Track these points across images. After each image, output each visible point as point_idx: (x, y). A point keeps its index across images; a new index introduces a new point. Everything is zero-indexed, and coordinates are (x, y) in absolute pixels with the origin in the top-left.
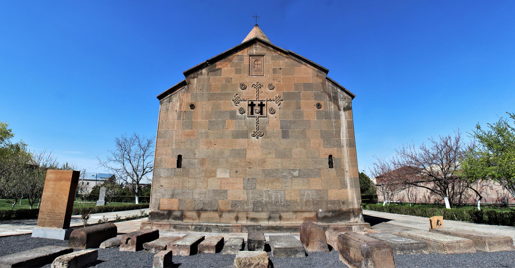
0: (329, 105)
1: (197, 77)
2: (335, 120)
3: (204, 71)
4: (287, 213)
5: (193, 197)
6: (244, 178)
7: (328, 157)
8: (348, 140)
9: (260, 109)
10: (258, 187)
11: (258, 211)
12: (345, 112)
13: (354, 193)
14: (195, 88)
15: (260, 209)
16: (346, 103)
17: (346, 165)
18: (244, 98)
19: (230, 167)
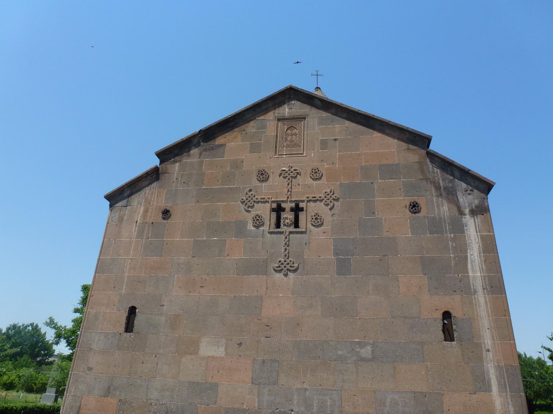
0: (438, 206)
1: (180, 161)
2: (452, 235)
3: (195, 151)
7: (441, 317)
8: (487, 278)
12: (473, 217)
13: (508, 404)
14: (175, 180)
16: (474, 199)
17: (485, 334)
18: (263, 197)
19: (228, 333)
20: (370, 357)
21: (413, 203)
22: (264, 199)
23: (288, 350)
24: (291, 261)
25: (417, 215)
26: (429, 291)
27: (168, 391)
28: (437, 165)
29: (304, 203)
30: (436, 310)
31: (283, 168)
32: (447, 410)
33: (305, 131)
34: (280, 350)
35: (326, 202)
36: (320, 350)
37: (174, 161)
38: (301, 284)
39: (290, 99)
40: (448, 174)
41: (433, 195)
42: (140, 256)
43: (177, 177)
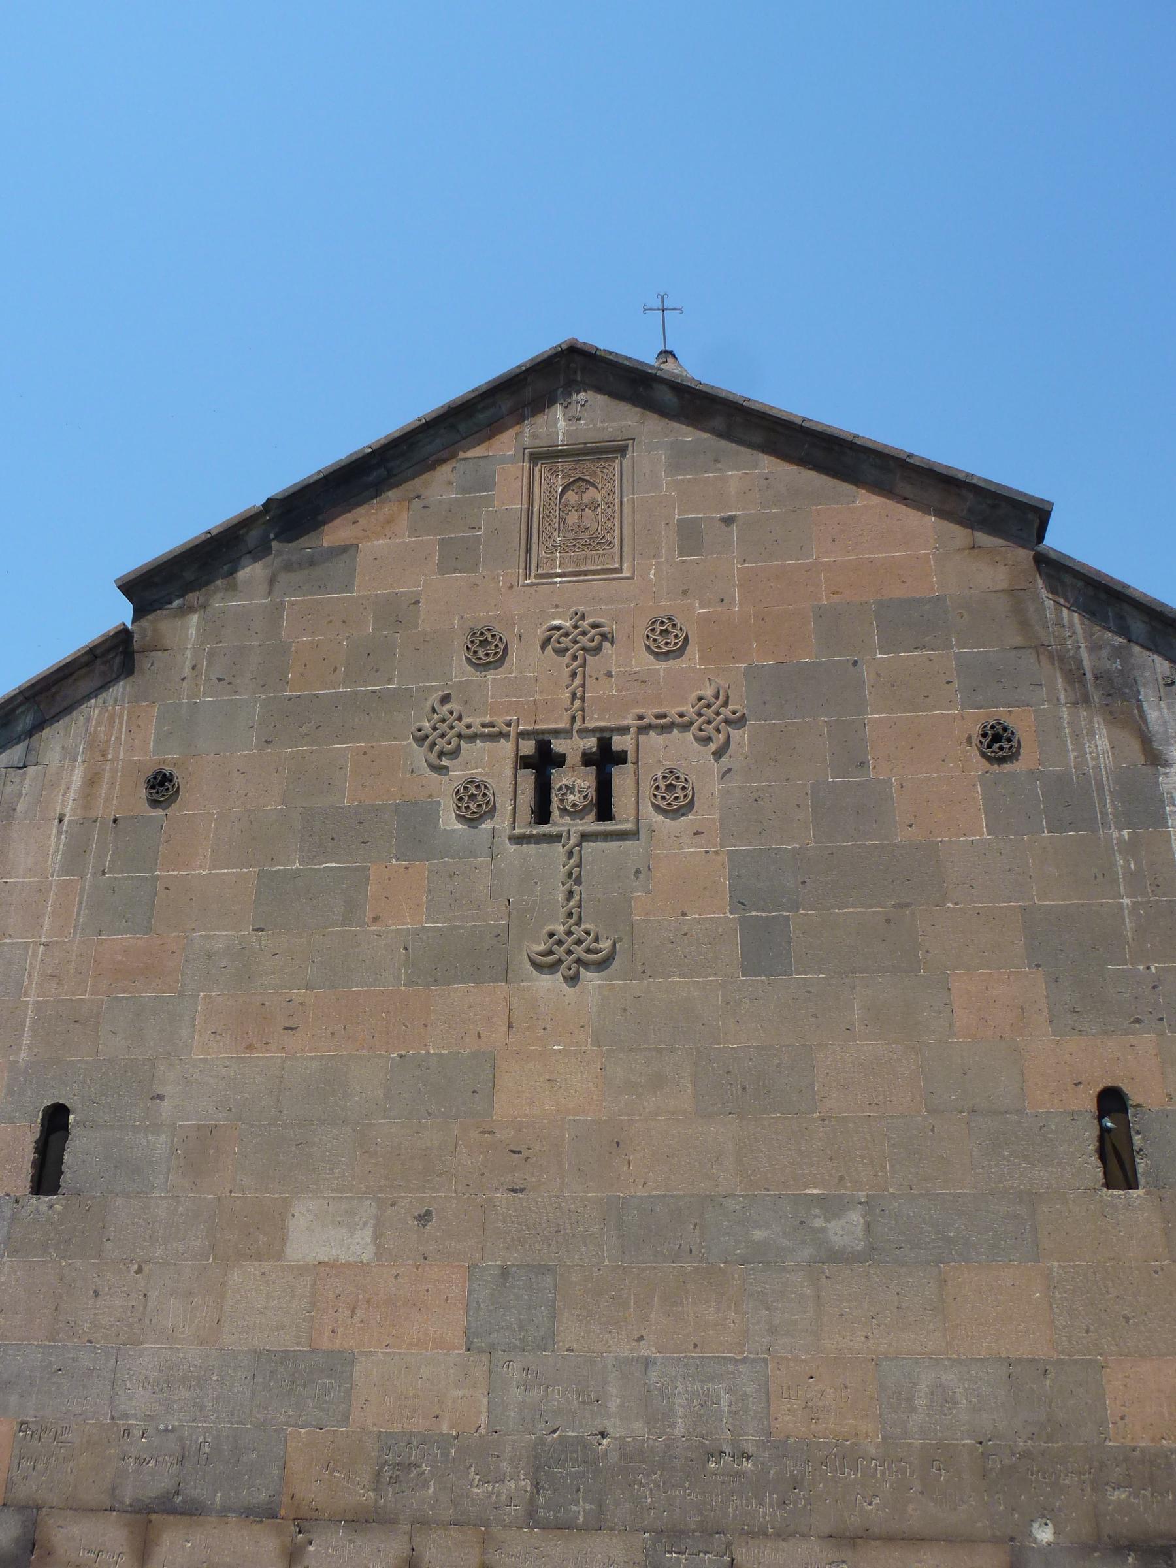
0: (1076, 736)
1: (204, 607)
2: (1125, 833)
3: (252, 572)
4: (783, 1544)
5: (111, 1405)
6: (473, 1266)
7: (1092, 1106)
9: (594, 785)
10: (569, 1333)
11: (564, 1527)
14: (187, 671)
15: (581, 1509)
18: (488, 720)
20: (860, 1246)
21: (993, 727)
22: (494, 726)
23: (587, 1231)
24: (588, 933)
25: (1008, 767)
26: (1051, 1021)
27: (183, 1387)
28: (1072, 601)
29: (629, 737)
30: (1076, 1084)
31: (554, 619)
32: (1118, 1420)
33: (624, 494)
34: (558, 1231)
35: (701, 730)
36: (692, 1227)
37: (181, 607)
38: (625, 1010)
39: (571, 387)
40: (1108, 629)
41: (1058, 699)
42: (75, 933)
43: (194, 663)
